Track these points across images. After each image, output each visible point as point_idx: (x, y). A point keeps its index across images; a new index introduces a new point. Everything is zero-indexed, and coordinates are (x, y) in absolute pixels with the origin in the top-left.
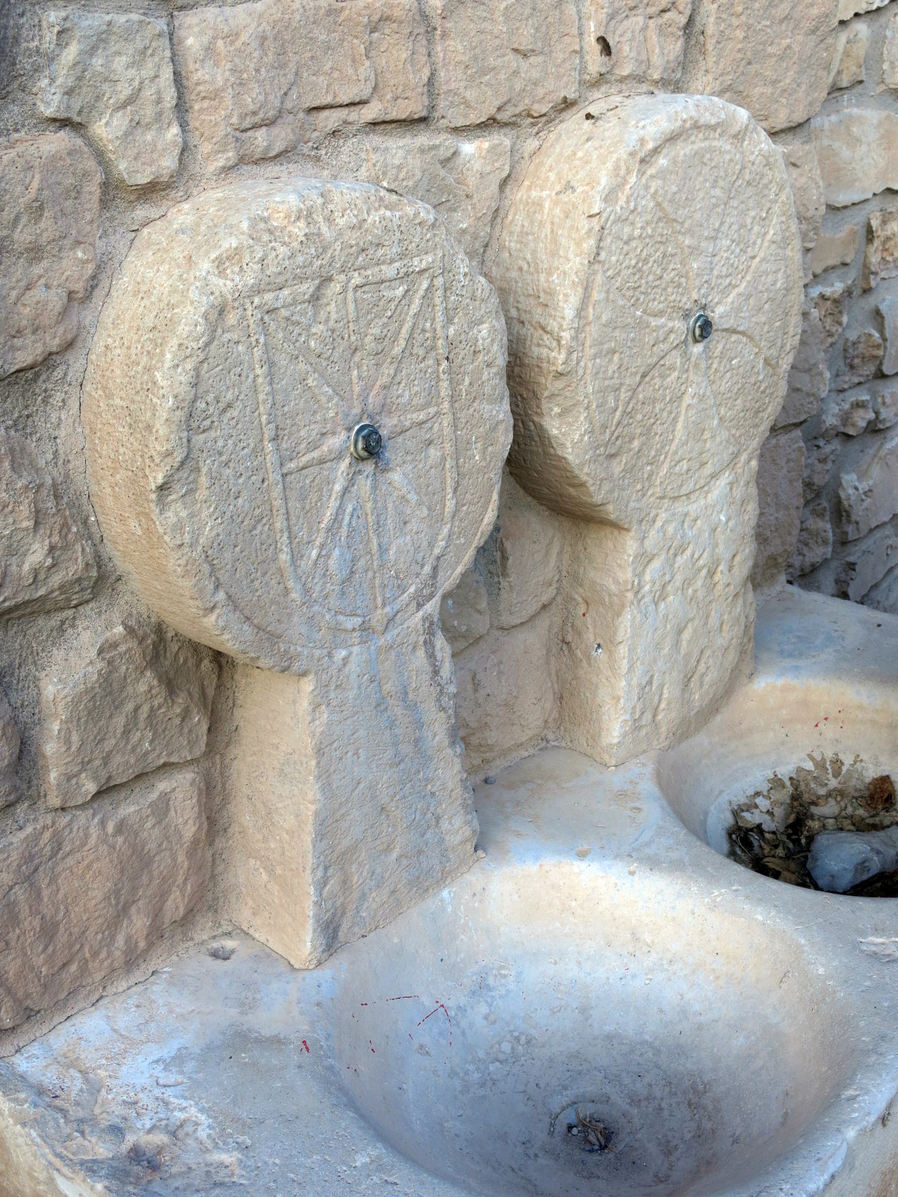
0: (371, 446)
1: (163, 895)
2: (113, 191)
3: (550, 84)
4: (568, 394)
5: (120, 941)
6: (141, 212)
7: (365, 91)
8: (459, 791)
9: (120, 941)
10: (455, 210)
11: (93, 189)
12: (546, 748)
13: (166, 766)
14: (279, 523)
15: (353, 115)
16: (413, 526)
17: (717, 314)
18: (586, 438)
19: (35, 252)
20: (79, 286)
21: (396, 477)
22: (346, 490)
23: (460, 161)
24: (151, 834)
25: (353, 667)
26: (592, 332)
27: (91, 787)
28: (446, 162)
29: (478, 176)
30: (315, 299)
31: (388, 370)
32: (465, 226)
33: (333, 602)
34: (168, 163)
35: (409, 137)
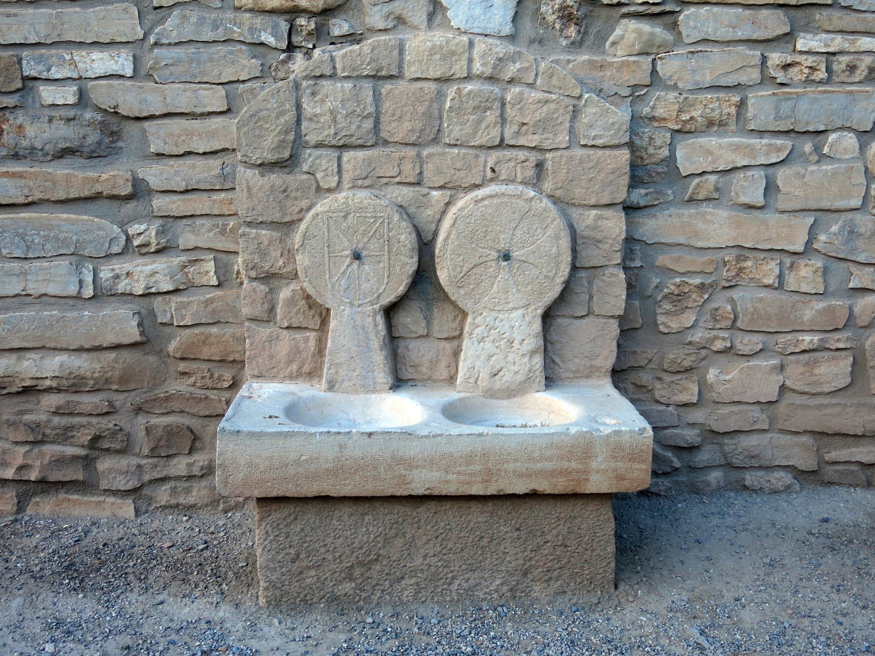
0: (357, 257)
1: (304, 364)
2: (319, 189)
3: (469, 179)
5: (289, 370)
6: (327, 195)
7: (395, 174)
8: (382, 366)
9: (289, 370)
11: (314, 187)
13: (306, 328)
14: (327, 267)
15: (392, 180)
16: (371, 282)
17: (515, 254)
19: (296, 199)
20: (305, 208)
21: (367, 267)
22: (348, 266)
24: (302, 346)
25: (346, 312)
26: (450, 247)
27: (286, 325)
28: (424, 196)
30: (345, 217)
31: (366, 240)
33: (342, 293)
34: (334, 185)
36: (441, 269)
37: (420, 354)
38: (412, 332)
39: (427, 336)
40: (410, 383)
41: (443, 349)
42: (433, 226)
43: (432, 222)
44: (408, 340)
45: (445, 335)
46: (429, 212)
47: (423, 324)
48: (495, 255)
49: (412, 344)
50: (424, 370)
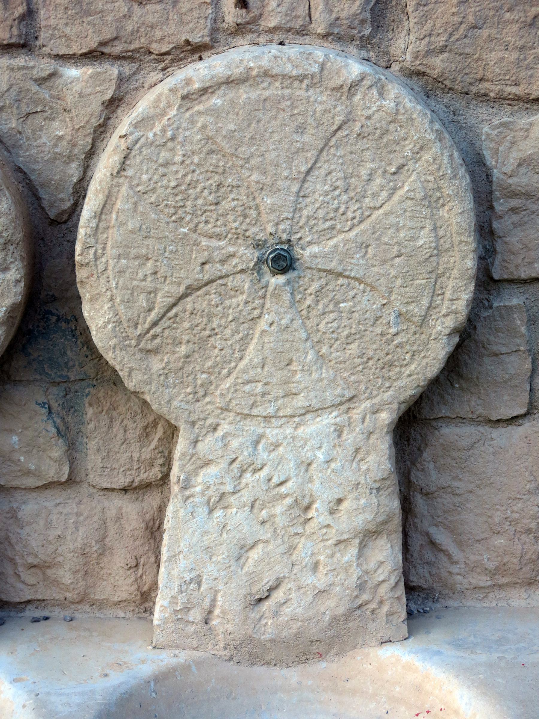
3: (171, 28)
4: (92, 283)
10: (53, 119)
12: (145, 619)
17: (306, 253)
18: (110, 326)
23: (59, 82)
26: (114, 235)
28: (41, 81)
29: (77, 95)
32: (61, 133)
35: (7, 57)
36: (93, 300)
37: (53, 534)
38: (28, 473)
39: (71, 481)
40: (31, 612)
41: (118, 518)
42: (74, 171)
43: (70, 158)
44: (18, 495)
45: (122, 481)
46: (59, 129)
47: (57, 451)
48: (247, 255)
49: (29, 507)
50: (67, 578)
